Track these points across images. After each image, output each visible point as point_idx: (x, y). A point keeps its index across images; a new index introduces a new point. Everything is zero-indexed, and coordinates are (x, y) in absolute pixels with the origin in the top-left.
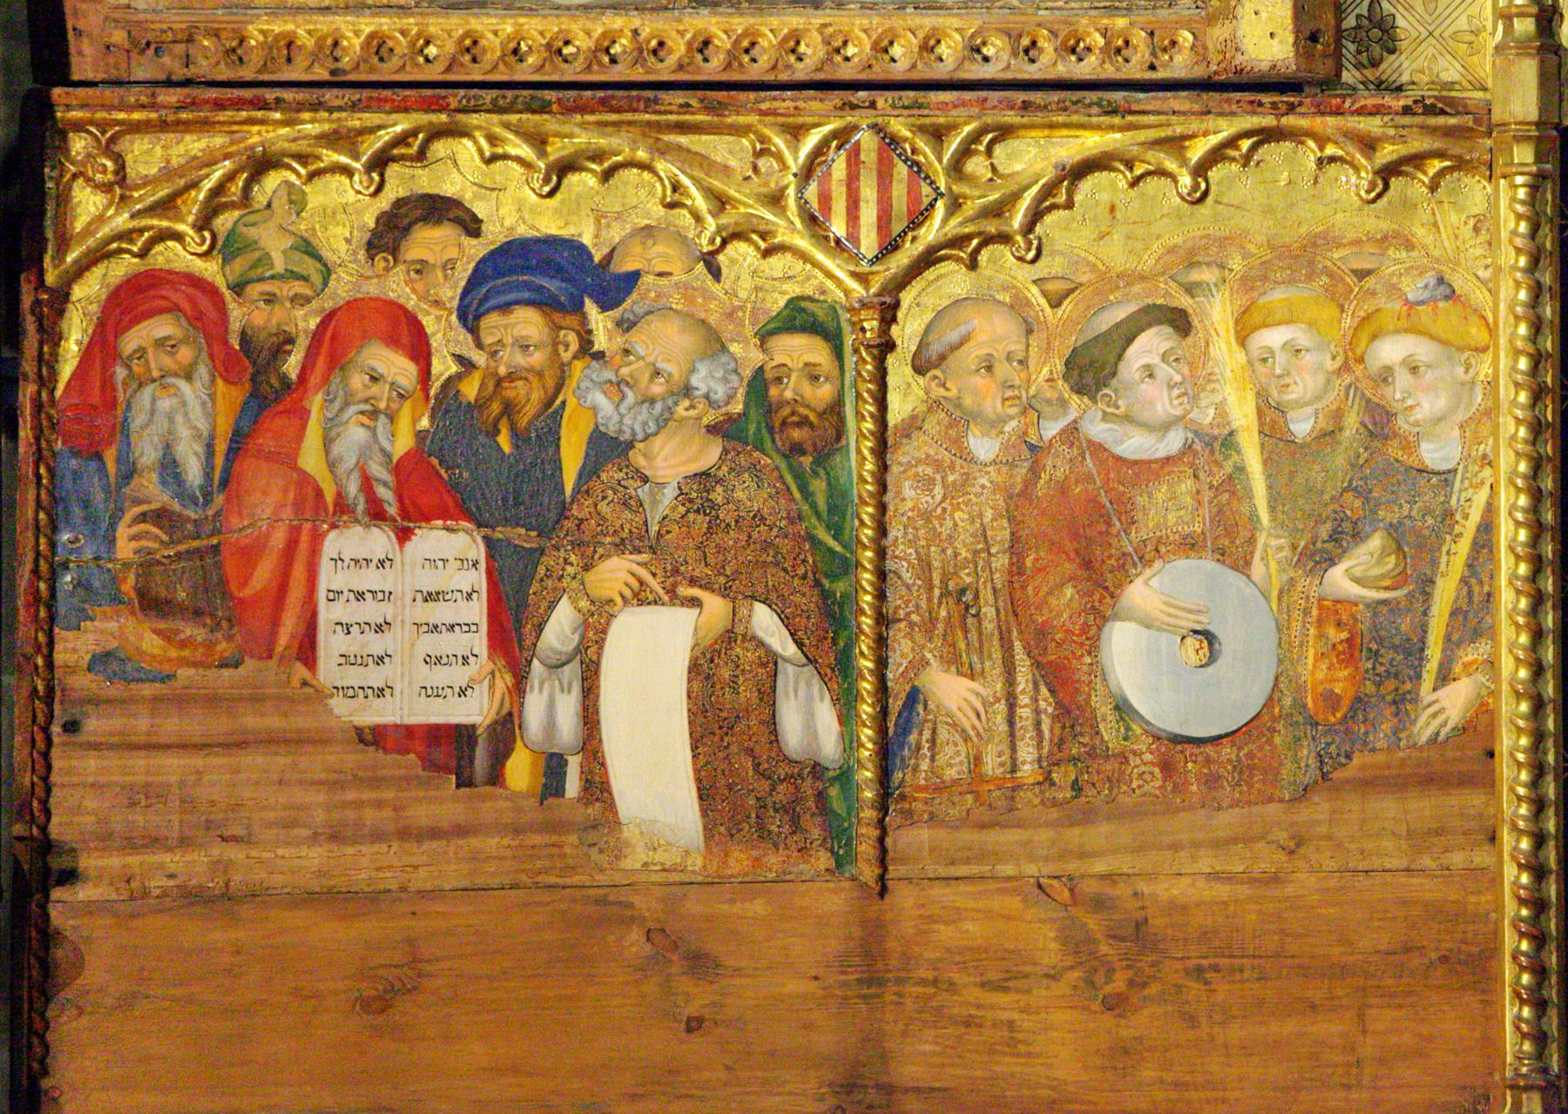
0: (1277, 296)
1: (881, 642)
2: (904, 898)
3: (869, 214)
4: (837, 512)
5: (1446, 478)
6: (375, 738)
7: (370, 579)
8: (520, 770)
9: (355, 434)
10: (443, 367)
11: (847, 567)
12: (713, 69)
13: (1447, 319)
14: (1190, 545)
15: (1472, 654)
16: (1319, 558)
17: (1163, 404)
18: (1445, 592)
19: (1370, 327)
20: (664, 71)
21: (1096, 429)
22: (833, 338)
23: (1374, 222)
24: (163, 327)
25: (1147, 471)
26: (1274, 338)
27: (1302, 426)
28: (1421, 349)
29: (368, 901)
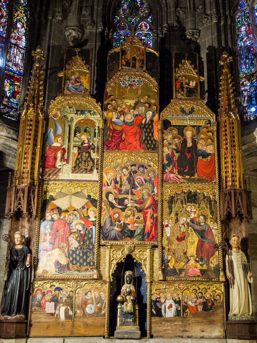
1: (74, 308)
3: (75, 286)
6: (48, 314)
7: (49, 305)
8: (55, 315)
9: (48, 297)
10: (53, 294)
11: (73, 304)
12: (68, 278)
13: (104, 291)
14: (91, 303)
15: (105, 309)
18: (103, 306)
19: (100, 292)
20: (65, 278)
21: (86, 297)
22: (73, 292)
23: (101, 287)
24: (39, 291)
26: (95, 292)
27: (97, 297)
28: (103, 293)
29: (47, 322)
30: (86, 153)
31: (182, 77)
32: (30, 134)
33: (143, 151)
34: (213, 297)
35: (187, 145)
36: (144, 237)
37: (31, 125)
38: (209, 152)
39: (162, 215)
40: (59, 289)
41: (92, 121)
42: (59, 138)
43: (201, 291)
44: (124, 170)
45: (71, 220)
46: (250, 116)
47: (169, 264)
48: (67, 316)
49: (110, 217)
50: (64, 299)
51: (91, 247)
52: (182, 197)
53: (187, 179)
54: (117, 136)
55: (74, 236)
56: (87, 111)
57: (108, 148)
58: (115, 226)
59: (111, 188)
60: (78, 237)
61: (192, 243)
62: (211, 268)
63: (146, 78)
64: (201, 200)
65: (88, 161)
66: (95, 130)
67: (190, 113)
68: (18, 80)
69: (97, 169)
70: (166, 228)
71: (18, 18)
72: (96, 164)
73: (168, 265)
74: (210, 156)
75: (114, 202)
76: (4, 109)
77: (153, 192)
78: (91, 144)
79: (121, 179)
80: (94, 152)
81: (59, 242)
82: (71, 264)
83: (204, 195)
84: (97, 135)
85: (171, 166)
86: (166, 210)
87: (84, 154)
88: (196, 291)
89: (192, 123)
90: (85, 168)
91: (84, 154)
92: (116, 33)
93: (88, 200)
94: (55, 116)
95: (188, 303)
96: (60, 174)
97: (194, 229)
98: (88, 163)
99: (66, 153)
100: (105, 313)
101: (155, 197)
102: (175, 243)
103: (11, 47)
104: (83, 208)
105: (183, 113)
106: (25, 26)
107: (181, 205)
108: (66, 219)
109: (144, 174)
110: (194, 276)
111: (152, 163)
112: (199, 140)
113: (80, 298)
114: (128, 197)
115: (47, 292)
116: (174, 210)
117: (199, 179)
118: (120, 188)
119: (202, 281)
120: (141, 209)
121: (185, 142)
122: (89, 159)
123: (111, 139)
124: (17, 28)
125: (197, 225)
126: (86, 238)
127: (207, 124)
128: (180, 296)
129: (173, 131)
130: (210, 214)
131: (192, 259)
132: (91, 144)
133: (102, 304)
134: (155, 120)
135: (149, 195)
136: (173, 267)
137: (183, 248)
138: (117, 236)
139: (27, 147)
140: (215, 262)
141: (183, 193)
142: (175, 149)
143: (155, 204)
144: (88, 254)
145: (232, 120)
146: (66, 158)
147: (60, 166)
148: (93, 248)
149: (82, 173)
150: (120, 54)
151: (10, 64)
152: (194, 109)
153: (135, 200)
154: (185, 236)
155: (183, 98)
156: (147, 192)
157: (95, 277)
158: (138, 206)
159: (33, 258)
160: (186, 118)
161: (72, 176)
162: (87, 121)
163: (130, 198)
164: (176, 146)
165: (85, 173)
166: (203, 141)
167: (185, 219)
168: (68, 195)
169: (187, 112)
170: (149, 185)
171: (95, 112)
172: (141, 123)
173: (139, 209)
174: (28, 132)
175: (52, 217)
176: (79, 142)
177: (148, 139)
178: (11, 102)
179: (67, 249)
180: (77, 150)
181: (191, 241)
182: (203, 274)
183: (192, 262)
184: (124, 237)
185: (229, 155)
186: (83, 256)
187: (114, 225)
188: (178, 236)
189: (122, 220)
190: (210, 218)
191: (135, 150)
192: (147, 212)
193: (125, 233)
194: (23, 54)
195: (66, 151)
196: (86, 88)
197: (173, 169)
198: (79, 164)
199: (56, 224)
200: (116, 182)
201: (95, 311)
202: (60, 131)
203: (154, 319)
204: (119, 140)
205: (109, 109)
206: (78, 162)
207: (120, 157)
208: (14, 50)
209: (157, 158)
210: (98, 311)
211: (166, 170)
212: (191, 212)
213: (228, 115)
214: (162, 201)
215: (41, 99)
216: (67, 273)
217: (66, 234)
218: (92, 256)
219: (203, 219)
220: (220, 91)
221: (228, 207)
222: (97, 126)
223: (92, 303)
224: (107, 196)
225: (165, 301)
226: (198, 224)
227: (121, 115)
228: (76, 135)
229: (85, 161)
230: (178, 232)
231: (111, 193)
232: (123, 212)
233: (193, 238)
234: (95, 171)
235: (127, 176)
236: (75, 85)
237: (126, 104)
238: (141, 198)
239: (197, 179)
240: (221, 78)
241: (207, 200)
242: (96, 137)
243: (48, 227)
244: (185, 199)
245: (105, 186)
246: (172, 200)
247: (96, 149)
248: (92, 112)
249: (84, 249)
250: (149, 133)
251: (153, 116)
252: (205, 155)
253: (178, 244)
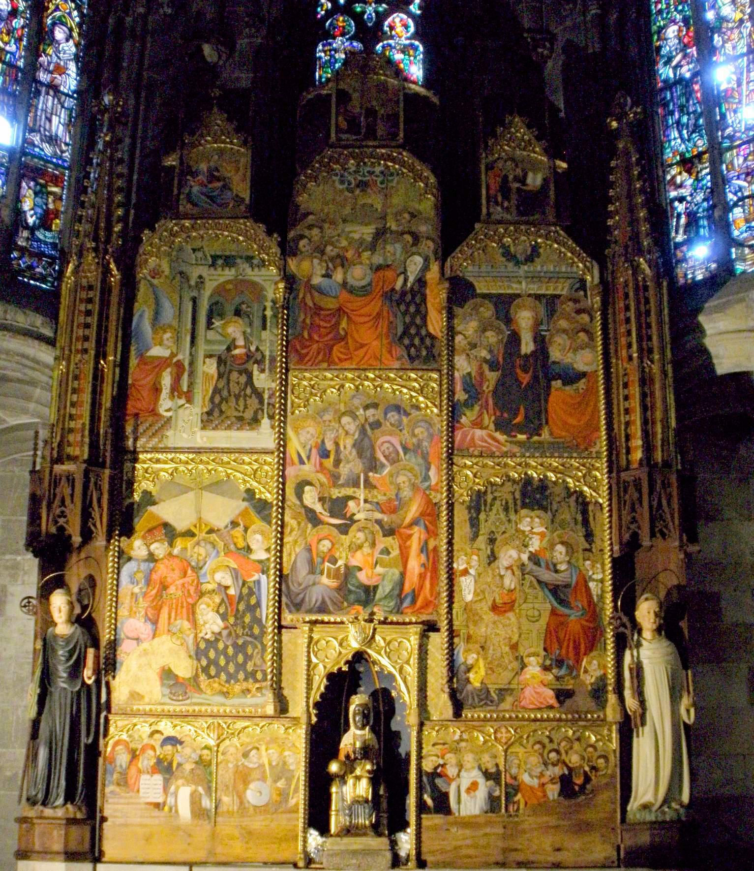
0: (271, 746)
2: (218, 827)
4: (211, 774)
5: (293, 771)
6: (148, 803)
7: (147, 782)
8: (166, 808)
9: (146, 762)
10: (158, 753)
14: (258, 780)
15: (296, 795)
16: (275, 781)
17: (255, 760)
18: (293, 787)
19: (283, 750)
21: (246, 764)
23: (284, 736)
25: (252, 769)
26: (271, 751)
27: (274, 763)
30: (240, 373)
31: (506, 161)
32: (87, 326)
33: (397, 365)
34: (589, 761)
35: (519, 350)
36: (402, 603)
37: (90, 301)
38: (581, 367)
39: (450, 543)
40: (172, 741)
41: (254, 285)
42: (165, 332)
43: (556, 747)
44: (346, 420)
45: (201, 558)
46: (695, 270)
47: (471, 675)
48: (198, 812)
49: (309, 550)
50: (188, 767)
51: (256, 631)
52: (505, 494)
53: (520, 444)
54: (325, 325)
55: (211, 603)
56: (241, 258)
57: (301, 358)
58: (322, 573)
59: (308, 470)
60: (220, 604)
62: (583, 684)
63: (403, 164)
65: (245, 395)
66: (265, 309)
67: (530, 259)
68: (56, 180)
69: (271, 417)
70: (463, 579)
71: (58, 14)
72: (269, 404)
74: (584, 380)
75: (318, 508)
76: (20, 258)
77: (427, 478)
78: (253, 348)
79: (337, 444)
80: (263, 371)
81: (170, 618)
82: (203, 677)
83: (568, 488)
84: (268, 324)
85: (477, 408)
86: (462, 529)
87: (234, 375)
88: (544, 747)
89: (534, 288)
90: (236, 414)
91: (234, 375)
92: (324, 45)
93: (246, 504)
94: (155, 273)
95: (520, 778)
96: (170, 433)
97: (539, 582)
98: (245, 400)
99: (185, 376)
100: (297, 805)
101: (433, 493)
102: (486, 621)
103: (38, 93)
104: (234, 524)
105: (508, 260)
106: (75, 35)
107: (502, 516)
108: (189, 554)
109: (401, 430)
110: (539, 709)
111: (421, 399)
112: (552, 336)
113: (231, 765)
114: (357, 495)
115: (143, 750)
116: (484, 529)
117: (552, 443)
118: (334, 469)
119: (560, 720)
120: (394, 526)
121: (514, 339)
122: (249, 391)
123: (309, 335)
124: (53, 41)
125: (548, 568)
126: (242, 607)
127: (576, 290)
128: (501, 761)
129: (482, 309)
131: (534, 663)
132: (253, 348)
133: (289, 781)
134: (432, 279)
135: (414, 487)
136: (482, 683)
137: (509, 632)
138: (327, 599)
139: (80, 361)
140: (595, 670)
141: (509, 481)
142: (486, 361)
143: (430, 513)
144: (250, 651)
145: (644, 279)
146: (185, 389)
147: (168, 410)
148: (263, 633)
149: (229, 428)
150: (334, 99)
151: (37, 139)
152: (540, 247)
153: (378, 503)
154: (514, 601)
155: (509, 217)
156: (410, 480)
157: (270, 710)
158: (386, 518)
159: (102, 661)
160: (517, 274)
161: (202, 438)
162: (242, 284)
163: (362, 498)
164: (491, 351)
165: (238, 429)
166: (565, 337)
167: (514, 553)
168: (192, 489)
169: (521, 258)
170: (413, 461)
171: (263, 261)
172: (393, 289)
173: (387, 527)
174: (82, 319)
175: (149, 550)
176: (220, 343)
177: (413, 331)
178: (39, 240)
179: (192, 636)
180: (215, 365)
181: (530, 613)
182: (561, 702)
183: (533, 670)
184: (345, 604)
185: (634, 378)
186: (236, 655)
187: (318, 571)
188: (494, 600)
189: (340, 558)
191: (375, 363)
192: (410, 536)
193: (350, 591)
194: (71, 110)
195: (184, 369)
196: (240, 194)
197: (480, 415)
198: (221, 402)
199: (162, 570)
200: (325, 454)
201: (271, 796)
202: (168, 313)
203: (428, 820)
204: (331, 336)
205: (303, 249)
206: (217, 400)
207: (333, 383)
208: (47, 101)
209: (435, 385)
210: (278, 799)
211: (464, 420)
212: (530, 536)
213: (632, 266)
214: (451, 507)
215: (117, 228)
216: (194, 700)
217: (190, 595)
218: (259, 656)
220: (610, 201)
221: (634, 520)
222: (269, 299)
223: (263, 779)
224: (299, 494)
225: (458, 775)
226: (551, 567)
227: (335, 268)
228: (213, 323)
229: (237, 397)
230: (494, 589)
231: (309, 483)
232: (343, 537)
234: (265, 422)
235: (353, 435)
236: (210, 186)
237: (351, 235)
238: (394, 497)
239: (549, 443)
240: (613, 163)
241: (577, 501)
242: (268, 328)
243: (140, 576)
244: (515, 499)
245: (293, 464)
246: (478, 503)
247: (267, 362)
248: (255, 261)
249: (237, 636)
250: (413, 317)
251: (426, 268)
252: (571, 377)
253: (494, 623)
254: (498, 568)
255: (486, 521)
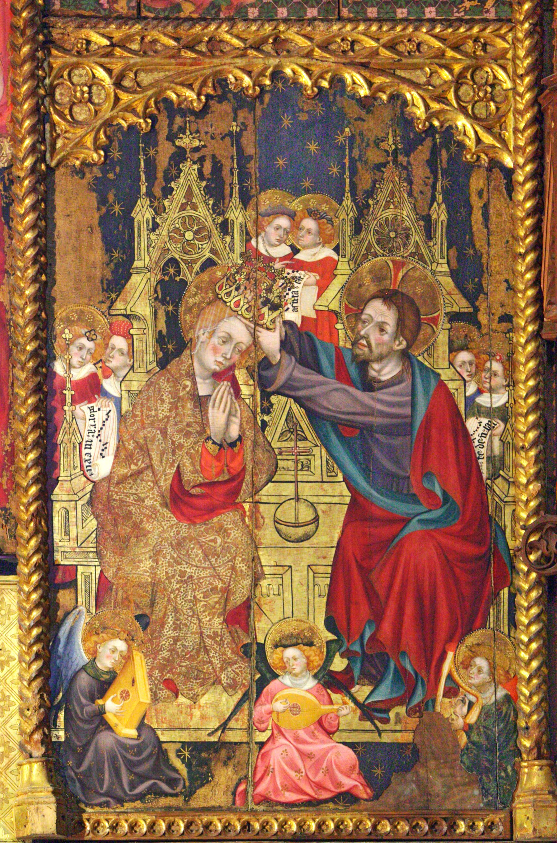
61: (300, 531)
64: (379, 167)
70: (83, 409)
73: (101, 712)
97: (313, 416)
102: (153, 539)
130: (448, 282)
131: (299, 666)
136: (141, 726)
141: (221, 99)
188: (178, 474)
190: (454, 317)
219: (390, 328)
226: (353, 371)
230: (178, 439)
233: (306, 490)
241: (432, 163)
253: (179, 545)
254: (192, 376)
255: (155, 227)
